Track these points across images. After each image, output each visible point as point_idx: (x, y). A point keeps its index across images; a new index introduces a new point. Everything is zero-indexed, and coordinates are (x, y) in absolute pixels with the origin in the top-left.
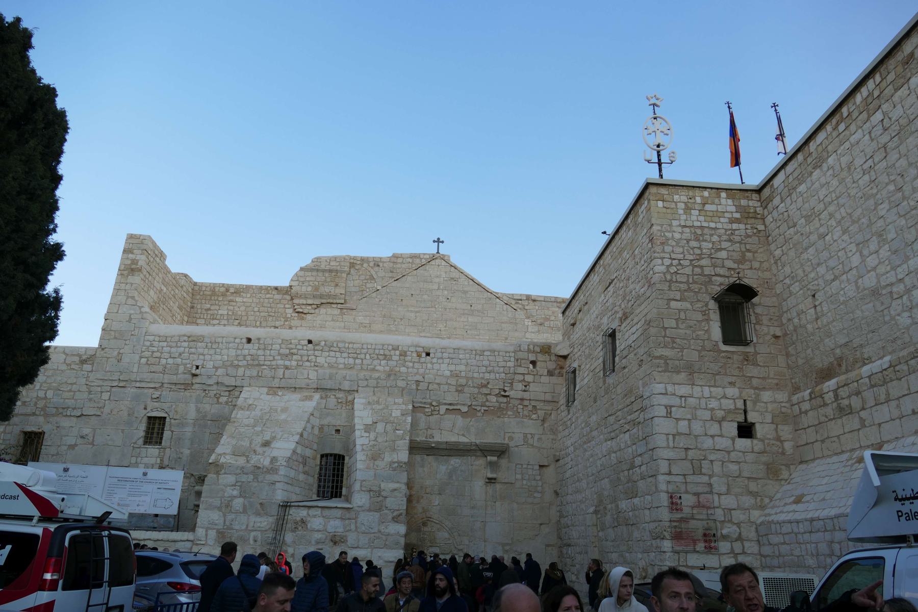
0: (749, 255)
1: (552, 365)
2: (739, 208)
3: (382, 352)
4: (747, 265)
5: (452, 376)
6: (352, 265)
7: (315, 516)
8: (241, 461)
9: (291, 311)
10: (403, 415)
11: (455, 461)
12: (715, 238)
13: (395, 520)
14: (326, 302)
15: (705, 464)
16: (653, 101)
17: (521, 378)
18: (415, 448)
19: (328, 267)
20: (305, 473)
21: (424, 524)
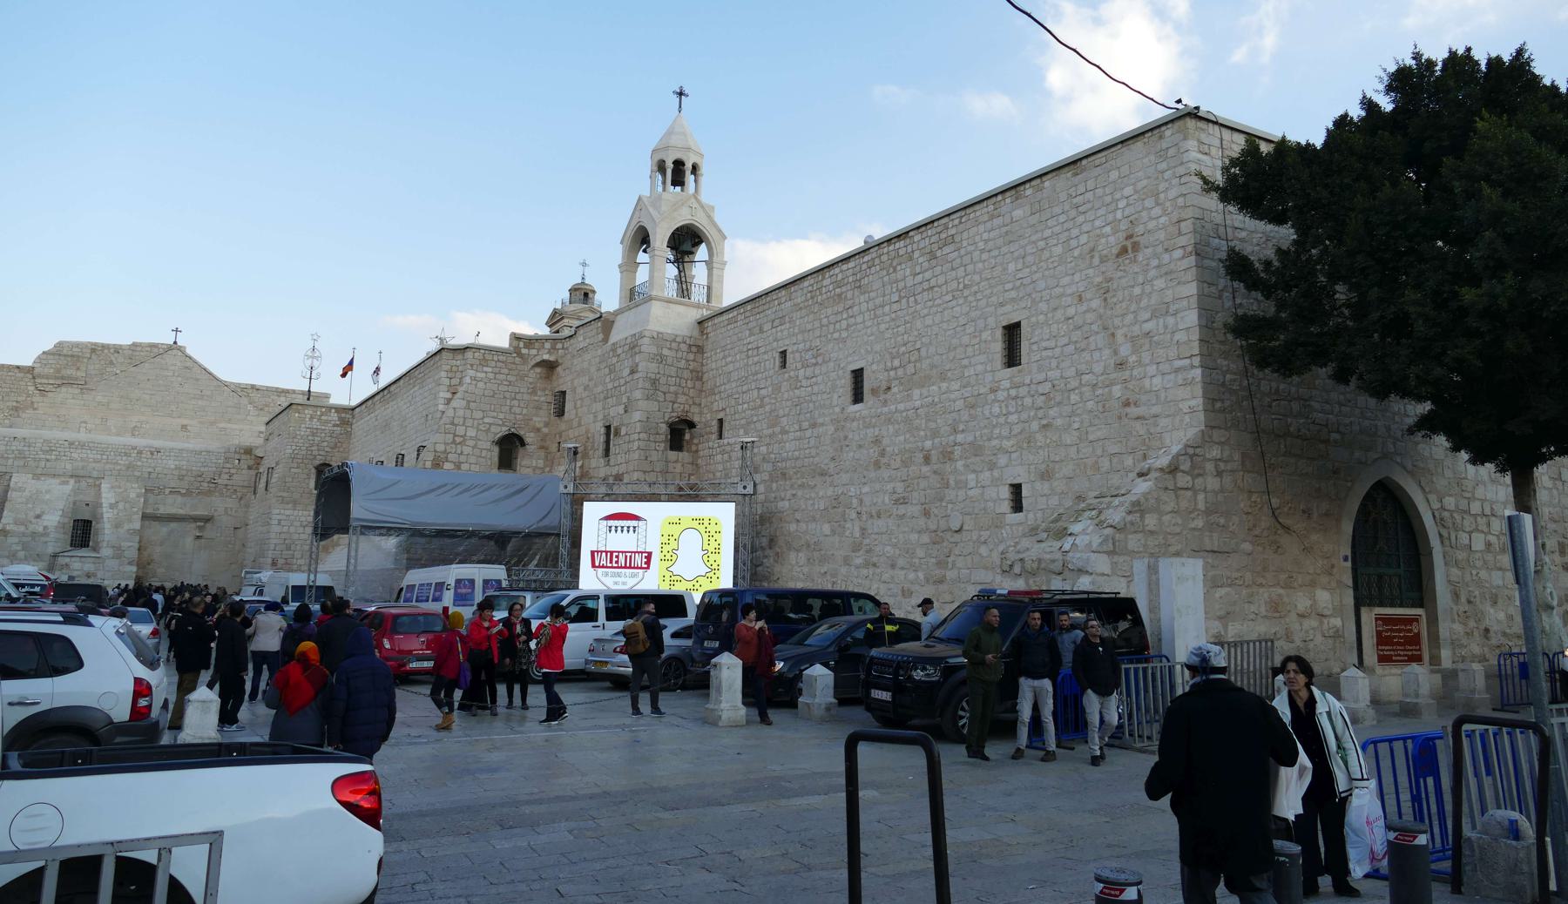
0: (339, 444)
1: (251, 463)
2: (340, 419)
3: (123, 451)
4: (337, 450)
5: (176, 469)
6: (93, 351)
7: (75, 562)
8: (22, 529)
9: (33, 388)
10: (137, 497)
11: (173, 525)
12: (323, 435)
13: (130, 563)
14: (67, 382)
15: (293, 547)
16: (315, 337)
17: (227, 470)
18: (145, 517)
19: (70, 353)
20: (64, 533)
21: (149, 564)
